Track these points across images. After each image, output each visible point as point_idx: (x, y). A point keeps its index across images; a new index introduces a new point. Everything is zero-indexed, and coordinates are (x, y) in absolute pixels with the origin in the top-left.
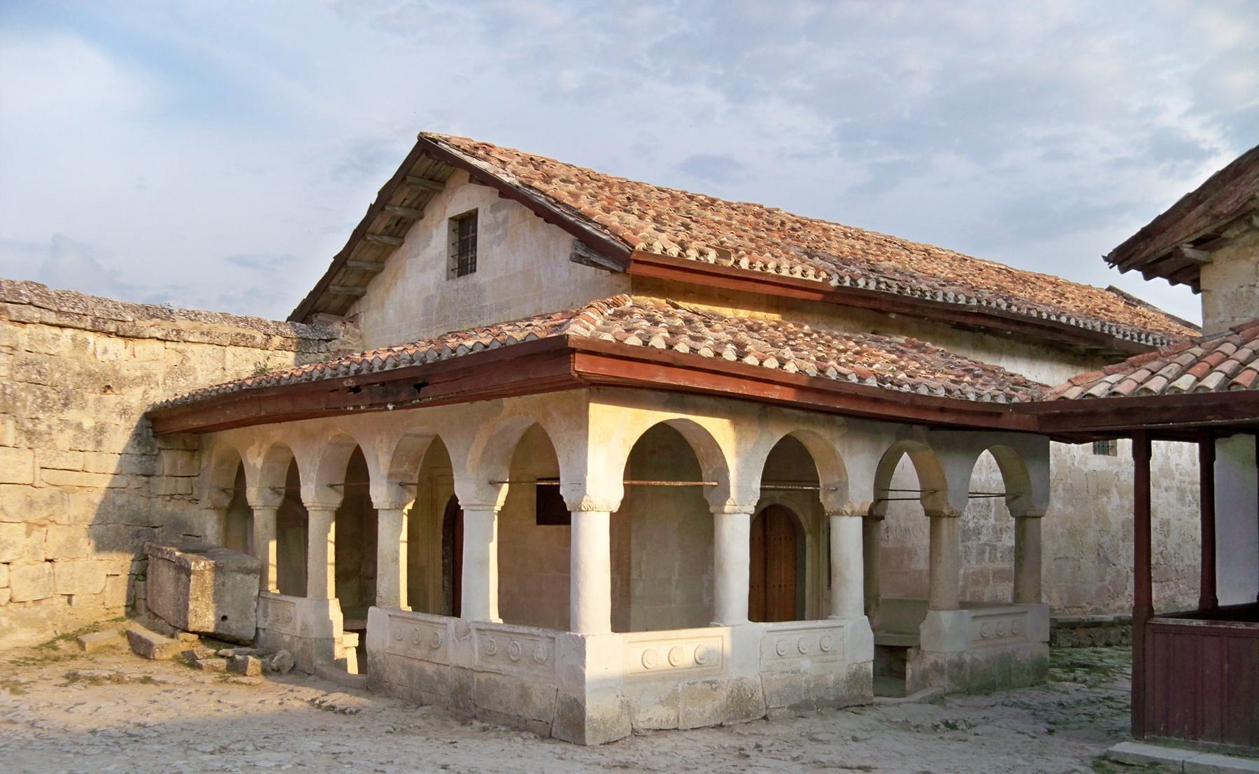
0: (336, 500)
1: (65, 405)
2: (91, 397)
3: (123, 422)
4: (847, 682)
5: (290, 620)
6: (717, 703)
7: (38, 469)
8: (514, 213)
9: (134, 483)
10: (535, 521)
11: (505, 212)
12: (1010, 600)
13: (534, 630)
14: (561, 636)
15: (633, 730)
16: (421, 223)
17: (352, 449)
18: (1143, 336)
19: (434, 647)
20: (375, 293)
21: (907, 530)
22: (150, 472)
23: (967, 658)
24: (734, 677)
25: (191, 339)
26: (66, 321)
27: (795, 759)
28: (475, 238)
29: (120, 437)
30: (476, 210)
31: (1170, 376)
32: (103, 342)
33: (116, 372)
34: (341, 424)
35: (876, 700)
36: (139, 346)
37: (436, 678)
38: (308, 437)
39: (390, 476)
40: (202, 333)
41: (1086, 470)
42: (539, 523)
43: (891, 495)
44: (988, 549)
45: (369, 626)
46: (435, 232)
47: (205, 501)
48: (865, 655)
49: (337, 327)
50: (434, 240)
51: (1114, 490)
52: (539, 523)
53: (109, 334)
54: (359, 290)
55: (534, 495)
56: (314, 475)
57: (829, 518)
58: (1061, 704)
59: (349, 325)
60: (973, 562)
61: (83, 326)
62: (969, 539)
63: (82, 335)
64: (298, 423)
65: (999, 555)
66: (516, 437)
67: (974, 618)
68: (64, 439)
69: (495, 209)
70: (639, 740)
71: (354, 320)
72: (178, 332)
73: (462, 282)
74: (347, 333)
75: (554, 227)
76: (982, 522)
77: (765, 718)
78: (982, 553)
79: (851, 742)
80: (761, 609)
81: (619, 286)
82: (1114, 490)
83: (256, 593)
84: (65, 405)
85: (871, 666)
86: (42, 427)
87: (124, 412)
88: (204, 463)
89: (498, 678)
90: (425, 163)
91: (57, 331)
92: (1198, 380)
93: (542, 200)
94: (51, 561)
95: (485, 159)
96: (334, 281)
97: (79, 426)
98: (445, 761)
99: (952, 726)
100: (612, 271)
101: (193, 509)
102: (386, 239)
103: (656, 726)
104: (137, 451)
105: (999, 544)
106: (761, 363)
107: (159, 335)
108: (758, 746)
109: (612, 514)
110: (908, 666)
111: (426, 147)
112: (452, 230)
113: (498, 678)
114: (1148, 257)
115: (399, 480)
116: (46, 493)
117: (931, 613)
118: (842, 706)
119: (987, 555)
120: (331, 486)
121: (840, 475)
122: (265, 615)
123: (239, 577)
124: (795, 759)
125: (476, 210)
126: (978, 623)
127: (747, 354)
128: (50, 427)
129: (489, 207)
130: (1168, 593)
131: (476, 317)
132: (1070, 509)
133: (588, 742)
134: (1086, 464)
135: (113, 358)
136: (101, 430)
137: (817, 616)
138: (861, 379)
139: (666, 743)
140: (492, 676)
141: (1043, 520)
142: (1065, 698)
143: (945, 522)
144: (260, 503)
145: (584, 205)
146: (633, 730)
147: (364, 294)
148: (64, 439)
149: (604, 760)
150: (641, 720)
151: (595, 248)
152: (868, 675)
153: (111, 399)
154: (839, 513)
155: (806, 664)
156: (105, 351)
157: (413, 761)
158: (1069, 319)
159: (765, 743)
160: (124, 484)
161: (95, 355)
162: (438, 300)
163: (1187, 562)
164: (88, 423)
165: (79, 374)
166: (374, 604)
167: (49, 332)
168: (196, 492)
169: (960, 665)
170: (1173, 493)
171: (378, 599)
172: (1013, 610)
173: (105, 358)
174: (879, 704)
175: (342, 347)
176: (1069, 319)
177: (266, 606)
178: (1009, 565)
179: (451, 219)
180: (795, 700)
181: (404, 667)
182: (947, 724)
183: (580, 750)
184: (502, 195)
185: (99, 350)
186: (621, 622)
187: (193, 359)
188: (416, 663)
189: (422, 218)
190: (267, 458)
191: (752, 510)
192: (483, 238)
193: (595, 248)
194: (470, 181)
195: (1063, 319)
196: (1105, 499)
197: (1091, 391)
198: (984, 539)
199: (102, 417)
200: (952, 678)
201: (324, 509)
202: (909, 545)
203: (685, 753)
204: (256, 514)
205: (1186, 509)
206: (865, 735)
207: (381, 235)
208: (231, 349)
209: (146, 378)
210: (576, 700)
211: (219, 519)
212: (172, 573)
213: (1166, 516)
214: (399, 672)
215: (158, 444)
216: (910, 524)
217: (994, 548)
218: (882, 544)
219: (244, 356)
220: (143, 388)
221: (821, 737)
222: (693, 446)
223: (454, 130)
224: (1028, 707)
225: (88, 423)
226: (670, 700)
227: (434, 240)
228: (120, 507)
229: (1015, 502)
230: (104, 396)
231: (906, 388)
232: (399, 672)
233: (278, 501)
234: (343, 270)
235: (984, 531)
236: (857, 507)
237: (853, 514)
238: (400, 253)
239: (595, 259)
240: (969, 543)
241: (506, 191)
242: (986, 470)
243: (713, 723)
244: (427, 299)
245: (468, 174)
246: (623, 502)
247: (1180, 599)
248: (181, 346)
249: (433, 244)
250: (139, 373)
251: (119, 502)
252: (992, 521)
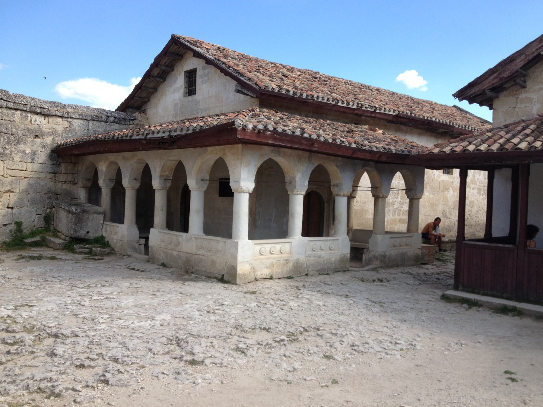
0: (137, 185)
1: (18, 142)
2: (29, 140)
3: (43, 150)
4: (339, 261)
5: (116, 233)
6: (288, 269)
7: (5, 169)
8: (211, 69)
9: (49, 176)
10: (218, 195)
11: (207, 70)
12: (405, 231)
13: (218, 238)
14: (229, 241)
15: (255, 279)
16: (173, 73)
17: (144, 165)
18: (467, 126)
19: (178, 244)
20: (153, 101)
21: (365, 202)
22: (55, 172)
23: (387, 254)
24: (295, 258)
25: (74, 116)
26: (18, 107)
27: (318, 291)
28: (196, 80)
29: (42, 156)
30: (196, 69)
31: (477, 145)
32: (35, 117)
33: (39, 128)
34: (141, 155)
35: (350, 269)
36: (51, 119)
37: (177, 257)
38: (124, 159)
39: (161, 176)
40: (79, 114)
41: (439, 180)
42: (220, 196)
43: (359, 188)
44: (397, 211)
45: (150, 236)
46: (178, 77)
47: (80, 184)
48: (347, 251)
49: (137, 114)
50: (178, 82)
51: (451, 189)
52: (220, 196)
53: (37, 114)
54: (146, 100)
55: (218, 185)
56: (128, 175)
57: (334, 197)
58: (425, 274)
59: (142, 114)
60: (391, 216)
61: (25, 109)
62: (390, 206)
63: (24, 114)
64: (121, 154)
65: (401, 213)
66: (212, 162)
67: (391, 238)
68: (17, 158)
69: (204, 68)
70: (257, 282)
71: (144, 112)
72: (68, 113)
73: (190, 98)
74: (141, 117)
75: (228, 78)
76: (395, 200)
77: (307, 275)
78: (395, 212)
79: (340, 285)
80: (306, 232)
82: (451, 189)
83: (102, 222)
84: (18, 142)
85: (349, 255)
86: (8, 152)
87: (44, 146)
88: (80, 169)
89: (202, 257)
90: (174, 47)
91: (14, 111)
92: (489, 146)
93: (224, 66)
94: (12, 208)
95: (199, 47)
96: (136, 95)
97: (24, 152)
98: (181, 290)
99: (381, 281)
100: (252, 97)
101: (75, 187)
102: (158, 79)
103: (264, 277)
104: (50, 163)
105: (402, 209)
106: (310, 136)
107: (59, 114)
108: (304, 286)
109: (250, 194)
110: (364, 256)
111: (175, 41)
112: (186, 77)
113: (202, 257)
114: (472, 94)
115: (164, 178)
116: (10, 179)
118: (336, 271)
119: (397, 213)
120: (135, 179)
122: (106, 231)
123: (95, 215)
124: (318, 291)
125: (196, 69)
126: (393, 240)
127: (305, 133)
128: (11, 152)
130: (472, 231)
131: (196, 113)
132: (432, 196)
133: (237, 282)
134: (439, 178)
135: (39, 123)
136: (34, 153)
137: (328, 235)
138: (350, 144)
139: (268, 283)
140: (200, 256)
142: (427, 271)
143: (380, 200)
144: (105, 186)
145: (241, 68)
146: (255, 279)
147: (149, 101)
148: (17, 158)
149: (245, 290)
150: (259, 274)
151: (244, 86)
152: (347, 259)
153: (38, 141)
154: (338, 195)
155: (323, 253)
156: (36, 120)
157: (167, 290)
158: (436, 119)
159: (307, 284)
160: (44, 176)
161: (31, 122)
163: (480, 218)
164: (28, 151)
165: (24, 130)
166: (152, 227)
167: (10, 112)
168: (76, 180)
169: (384, 256)
170: (475, 191)
171: (154, 225)
172: (407, 235)
173: (35, 123)
174: (352, 270)
175: (139, 123)
176: (436, 119)
177: (106, 228)
178: (406, 217)
179: (185, 72)
180: (319, 268)
181: (164, 252)
182: (379, 280)
183: (234, 286)
184: (207, 63)
185: (33, 120)
186: (251, 236)
187: (75, 125)
188: (169, 251)
189: (173, 70)
190: (107, 167)
191: (304, 193)
192: (199, 80)
193: (244, 86)
194: (194, 56)
195: (434, 119)
196: (447, 192)
197: (443, 150)
198: (396, 206)
199: (35, 148)
200: (381, 262)
201: (132, 189)
203: (276, 288)
204: (103, 190)
205: (481, 197)
206: (346, 283)
207: (156, 77)
208: (91, 123)
209: (54, 132)
210: (233, 266)
211: (86, 193)
212: (65, 214)
213: (473, 199)
214: (162, 254)
215: (60, 160)
216: (366, 200)
217: (400, 210)
218: (355, 208)
219: (97, 125)
220: (52, 136)
221: (329, 283)
222: (282, 168)
223: (187, 33)
224: (412, 274)
225: (28, 151)
226: (271, 266)
227: (178, 82)
228: (42, 186)
230: (35, 140)
231: (367, 148)
232: (162, 254)
233: (112, 185)
234: (140, 91)
235: (396, 203)
236: (346, 193)
237: (344, 196)
239: (245, 91)
240: (390, 208)
241: (209, 62)
242: (398, 181)
243: (286, 276)
244: (175, 104)
245: (192, 54)
246: (254, 189)
247: (476, 233)
248: (69, 120)
249: (178, 82)
250: (51, 130)
251: (42, 183)
252: (399, 199)
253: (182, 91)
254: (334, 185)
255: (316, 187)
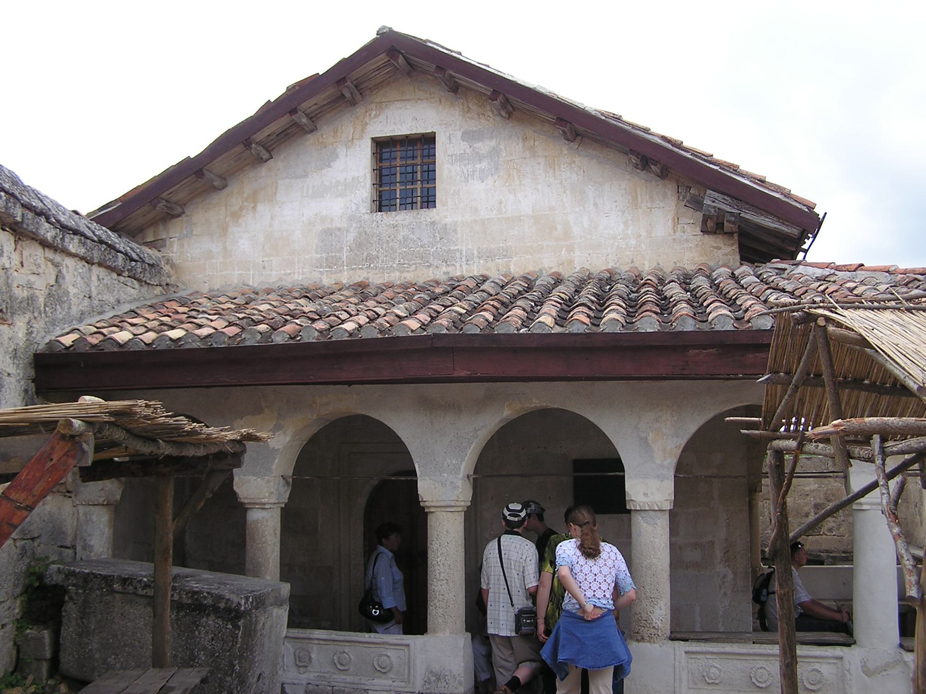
8: (508, 144)
11: (493, 143)
16: (311, 139)
46: (341, 151)
54: (179, 210)
73: (402, 218)
81: (719, 248)
129: (459, 134)
162: (351, 236)
204: (254, 515)
208: (96, 270)
220: (28, 315)
238: (263, 170)
248: (58, 258)
249: (338, 165)
253: (365, 191)
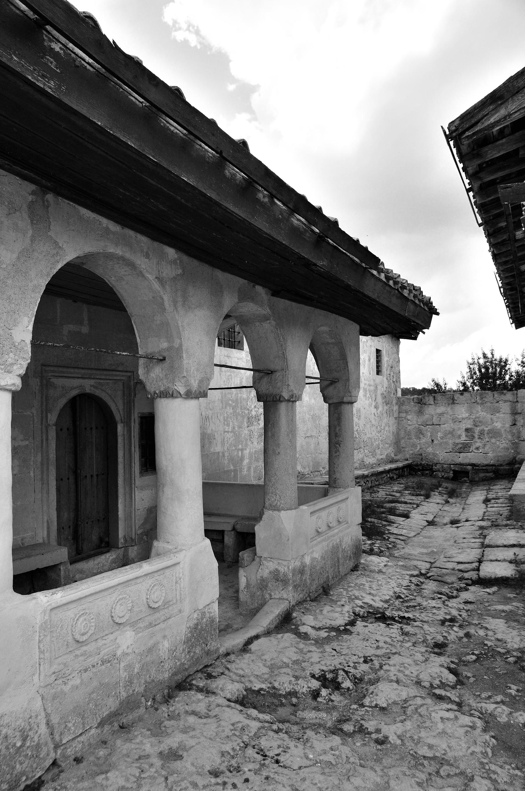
4: (187, 641)
57: (152, 402)
62: (252, 424)
85: (216, 606)
110: (242, 573)
114: (493, 125)
117: (268, 514)
121: (169, 338)
141: (355, 404)
143: (283, 407)
163: (368, 436)
202: (209, 431)
205: (367, 402)
229: (331, 388)
240: (252, 428)
254: (150, 358)
255: (92, 382)
